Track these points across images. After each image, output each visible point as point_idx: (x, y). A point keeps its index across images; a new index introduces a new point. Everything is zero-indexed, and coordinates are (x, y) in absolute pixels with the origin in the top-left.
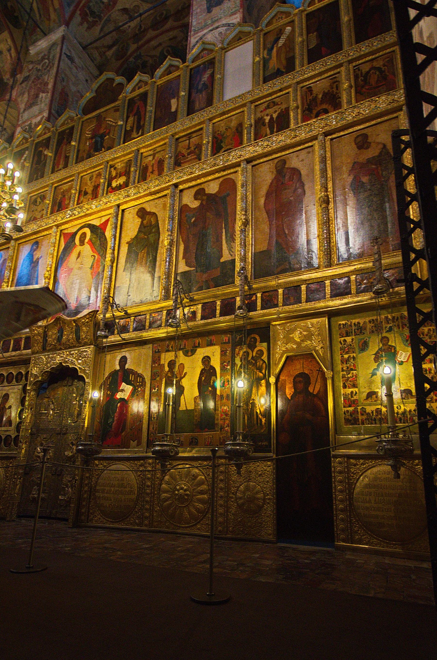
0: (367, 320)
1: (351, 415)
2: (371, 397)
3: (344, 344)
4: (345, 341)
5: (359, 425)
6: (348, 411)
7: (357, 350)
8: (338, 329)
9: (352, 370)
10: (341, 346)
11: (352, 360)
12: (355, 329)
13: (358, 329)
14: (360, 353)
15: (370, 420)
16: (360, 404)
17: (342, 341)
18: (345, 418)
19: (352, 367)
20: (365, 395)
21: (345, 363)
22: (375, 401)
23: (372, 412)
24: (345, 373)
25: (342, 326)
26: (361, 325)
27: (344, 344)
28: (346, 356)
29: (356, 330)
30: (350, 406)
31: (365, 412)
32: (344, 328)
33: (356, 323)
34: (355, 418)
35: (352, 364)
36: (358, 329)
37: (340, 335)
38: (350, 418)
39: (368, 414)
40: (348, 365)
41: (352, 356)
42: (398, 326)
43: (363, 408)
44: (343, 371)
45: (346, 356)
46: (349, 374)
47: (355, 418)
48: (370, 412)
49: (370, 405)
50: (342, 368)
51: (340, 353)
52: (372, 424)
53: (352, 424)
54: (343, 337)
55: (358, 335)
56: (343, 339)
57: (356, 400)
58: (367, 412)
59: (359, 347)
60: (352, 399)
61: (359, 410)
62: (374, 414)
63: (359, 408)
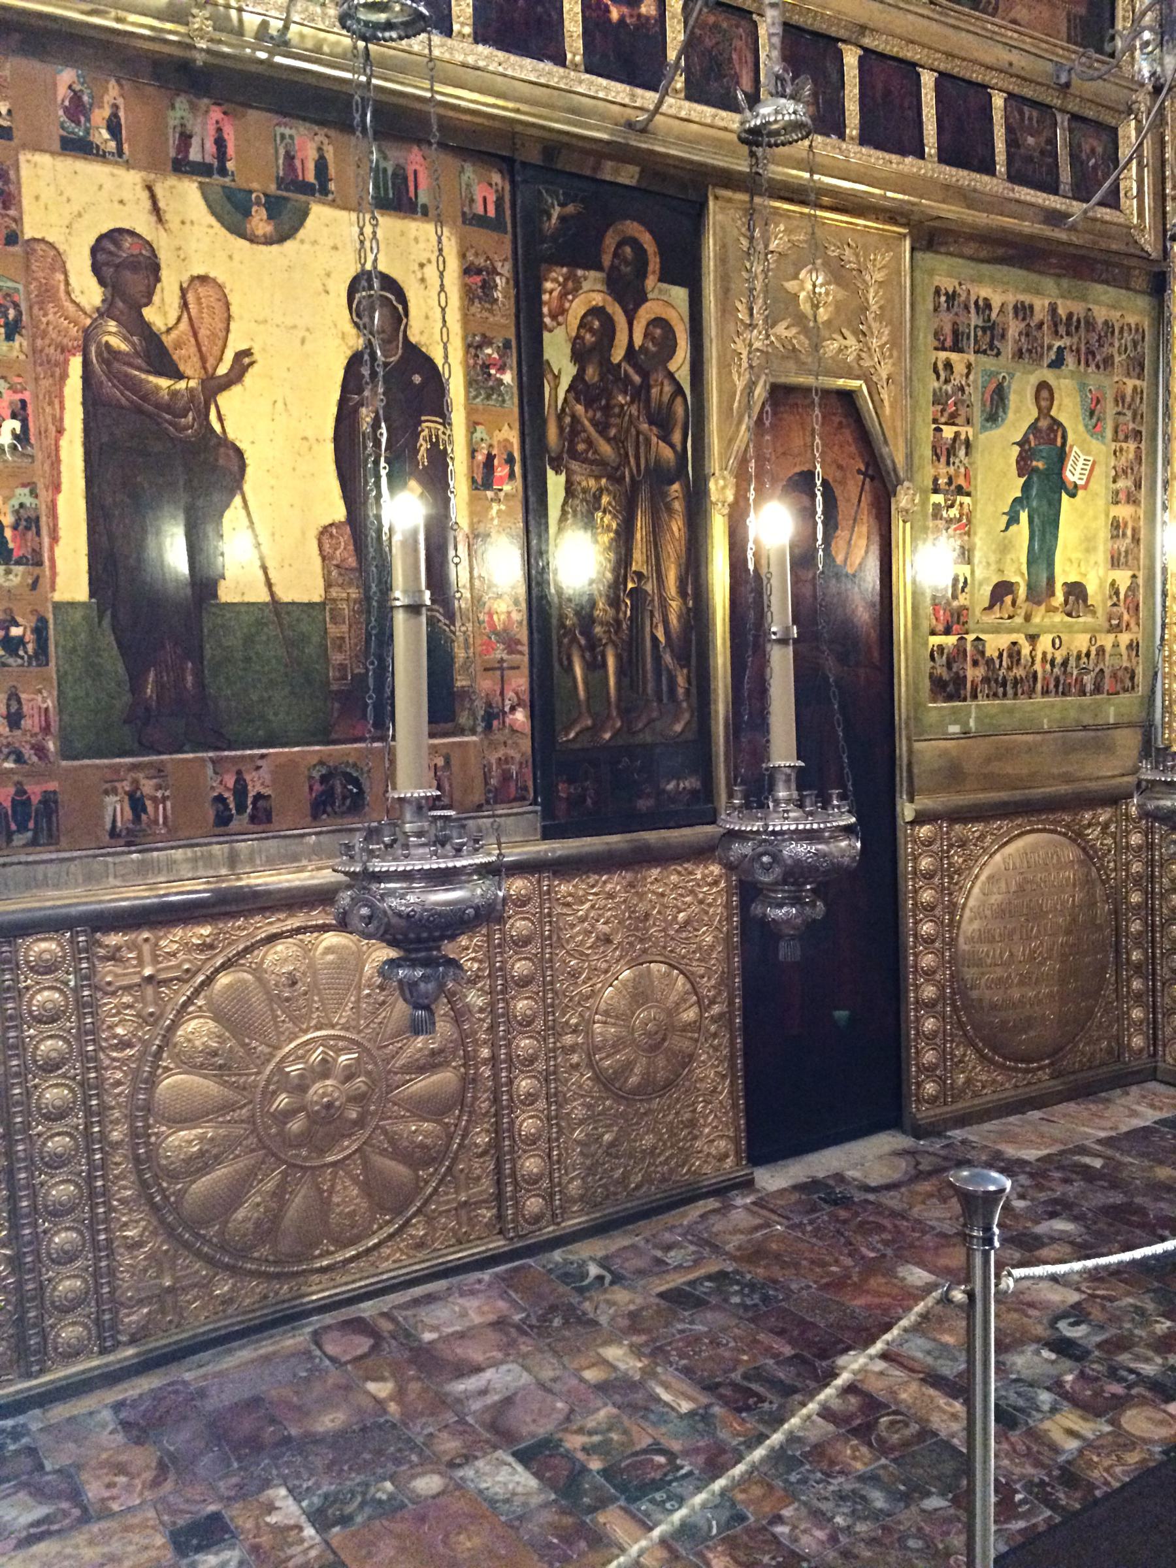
0: (1011, 298)
1: (949, 666)
2: (1002, 602)
3: (947, 381)
4: (948, 365)
5: (965, 700)
6: (941, 648)
7: (977, 416)
8: (931, 307)
9: (960, 491)
10: (936, 385)
11: (962, 453)
12: (976, 327)
13: (984, 329)
14: (984, 429)
15: (993, 684)
16: (971, 625)
17: (940, 366)
18: (931, 675)
19: (961, 481)
20: (987, 590)
21: (943, 459)
22: (1010, 617)
23: (1001, 656)
24: (938, 498)
25: (943, 299)
26: (994, 315)
27: (947, 381)
28: (948, 432)
29: (980, 333)
30: (947, 631)
31: (983, 653)
32: (948, 309)
33: (981, 303)
34: (957, 673)
35: (962, 470)
36: (984, 329)
37: (936, 335)
38: (946, 676)
39: (990, 662)
40: (952, 470)
41: (963, 437)
42: (1078, 350)
43: (978, 639)
44: (936, 490)
45: (948, 432)
46: (952, 506)
47: (957, 673)
48: (996, 654)
49: (996, 630)
50: (936, 480)
51: (931, 417)
52: (995, 695)
53: (950, 698)
54: (944, 349)
55: (985, 352)
56: (943, 355)
57: (965, 608)
58: (988, 654)
59: (984, 405)
60: (955, 604)
61: (969, 648)
62: (1004, 664)
63: (971, 637)
